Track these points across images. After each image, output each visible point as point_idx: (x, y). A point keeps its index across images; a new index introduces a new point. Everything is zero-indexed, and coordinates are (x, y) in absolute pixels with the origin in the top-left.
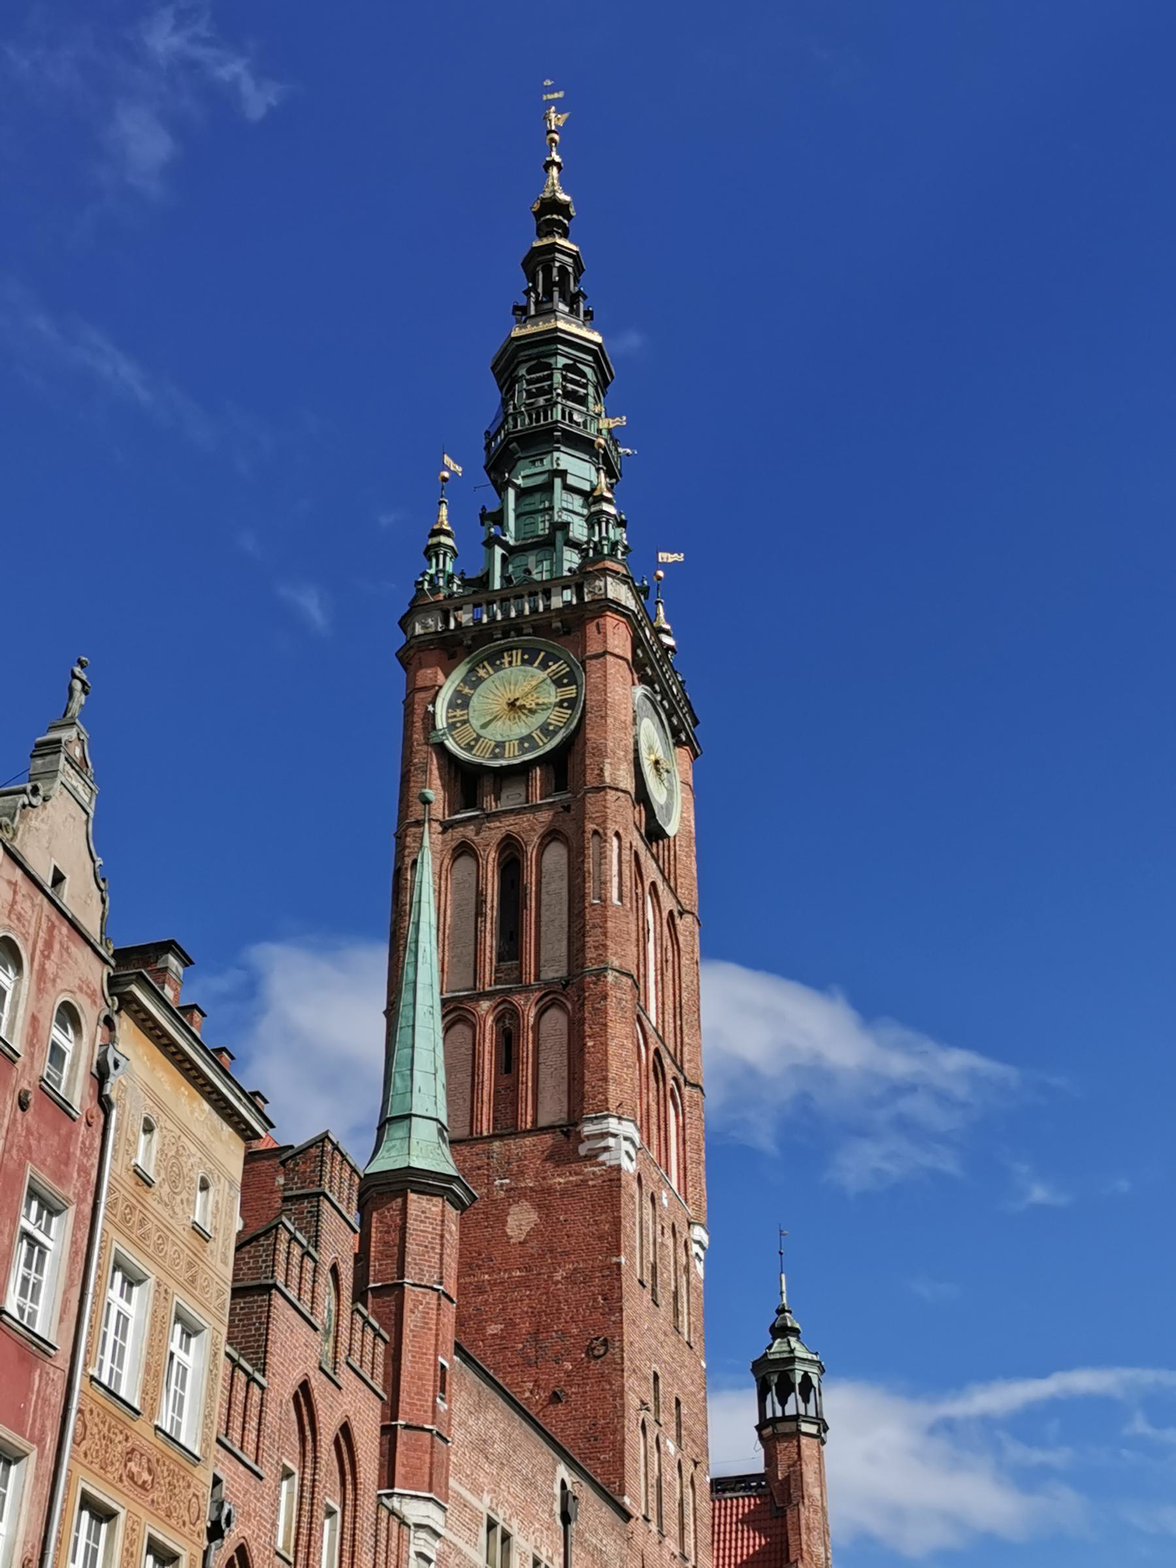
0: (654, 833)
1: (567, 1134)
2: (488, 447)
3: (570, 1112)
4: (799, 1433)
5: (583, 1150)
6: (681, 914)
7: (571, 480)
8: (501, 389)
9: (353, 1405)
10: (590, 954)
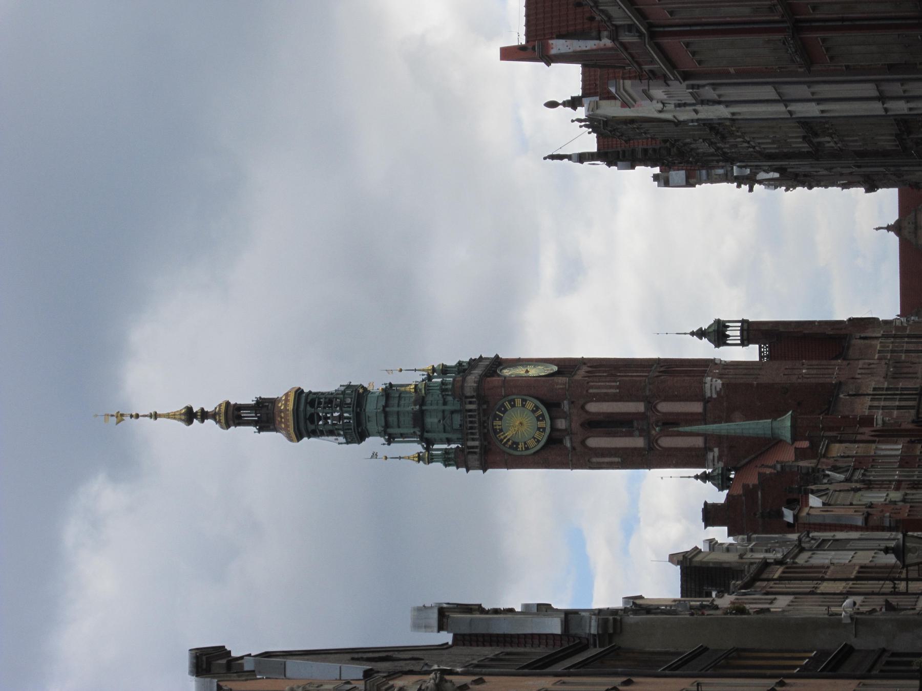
1: (708, 402)
2: (347, 443)
3: (698, 400)
4: (748, 330)
5: (715, 396)
6: (585, 364)
7: (383, 403)
8: (309, 437)
9: (866, 430)
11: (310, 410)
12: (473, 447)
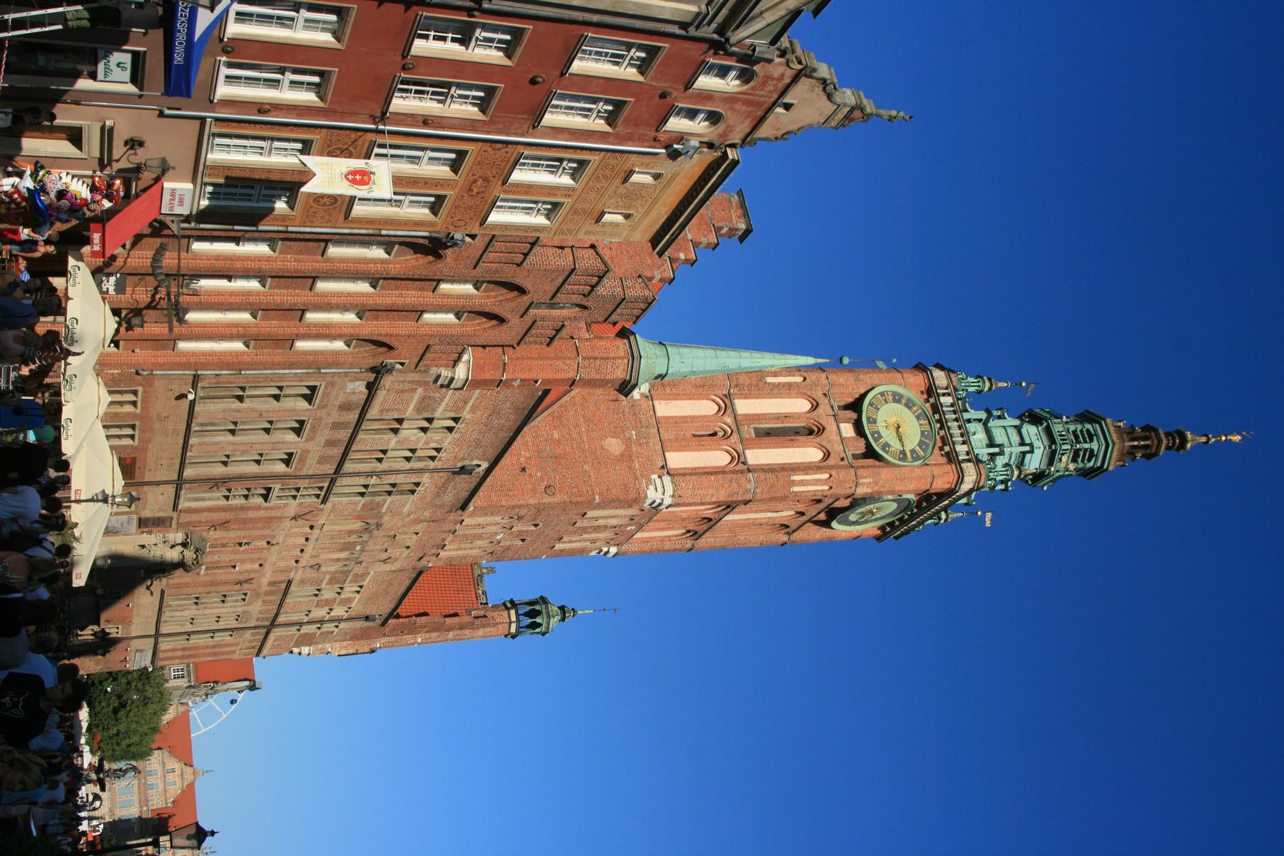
0: (833, 513)
1: (663, 467)
4: (511, 623)
7: (1028, 456)
10: (762, 476)
11: (1094, 445)
12: (944, 395)
